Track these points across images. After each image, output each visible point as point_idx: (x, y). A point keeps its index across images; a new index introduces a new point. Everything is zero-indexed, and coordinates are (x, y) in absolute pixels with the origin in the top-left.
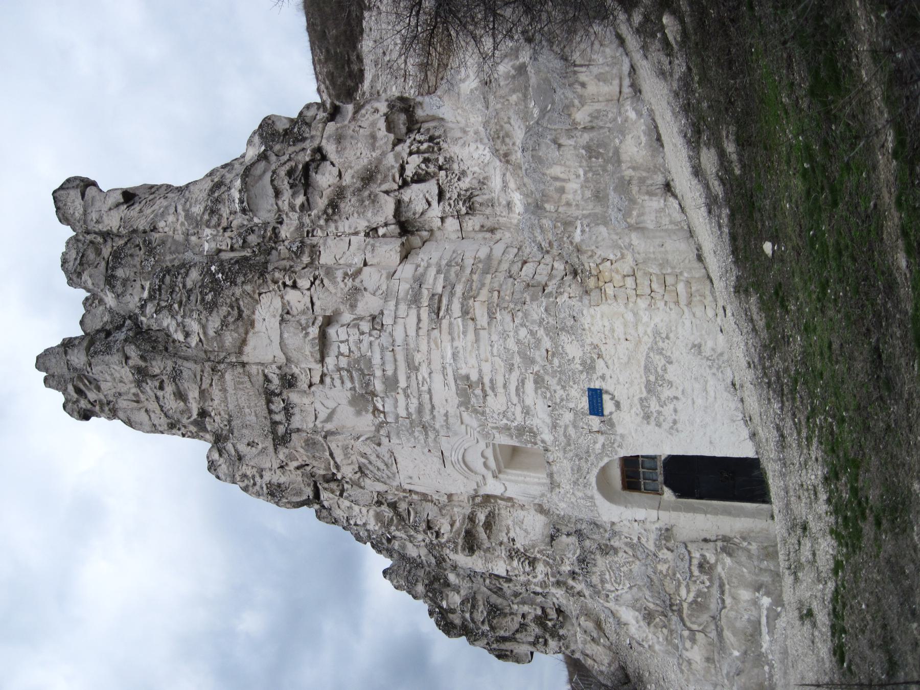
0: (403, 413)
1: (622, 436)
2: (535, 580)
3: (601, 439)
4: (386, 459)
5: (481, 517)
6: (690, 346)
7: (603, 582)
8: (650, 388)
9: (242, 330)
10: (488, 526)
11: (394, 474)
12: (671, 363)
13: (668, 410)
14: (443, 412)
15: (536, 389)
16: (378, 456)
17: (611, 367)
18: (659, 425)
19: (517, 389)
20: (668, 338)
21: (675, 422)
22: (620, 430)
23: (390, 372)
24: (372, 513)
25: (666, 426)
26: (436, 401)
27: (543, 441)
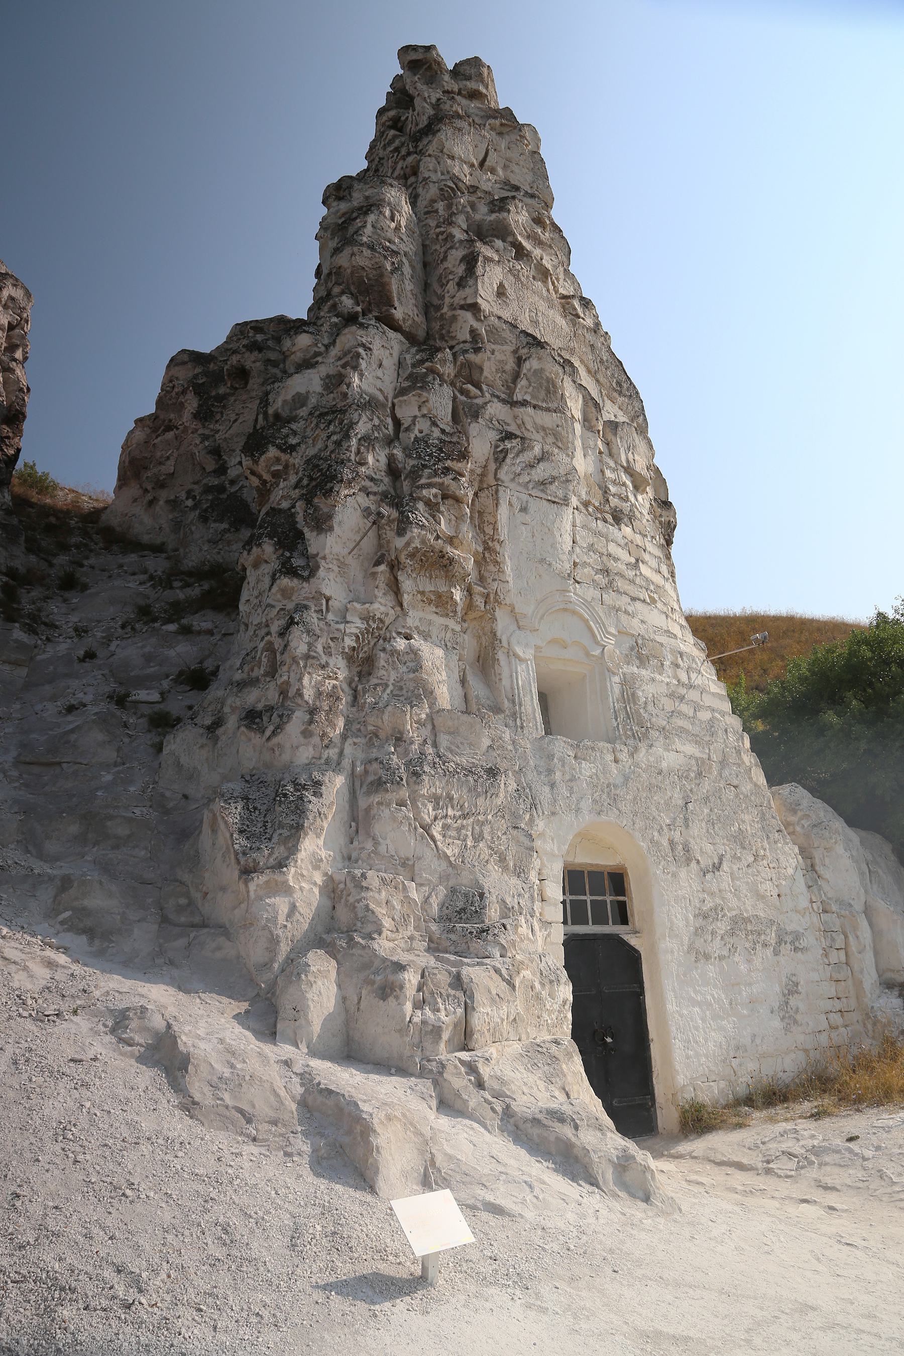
0: (612, 548)
1: (674, 875)
2: (320, 649)
3: (665, 843)
4: (553, 488)
5: (458, 595)
6: (794, 979)
7: (436, 800)
8: (739, 923)
9: (601, 379)
10: (442, 602)
11: (526, 485)
12: (776, 953)
13: (716, 947)
14: (630, 609)
15: (697, 759)
16: (554, 479)
17: (750, 871)
18: (698, 932)
19: (687, 731)
20: (796, 949)
21: (707, 957)
22: (683, 873)
23: (646, 557)
24: (381, 398)
25: (699, 943)
26: (638, 604)
27: (636, 749)
